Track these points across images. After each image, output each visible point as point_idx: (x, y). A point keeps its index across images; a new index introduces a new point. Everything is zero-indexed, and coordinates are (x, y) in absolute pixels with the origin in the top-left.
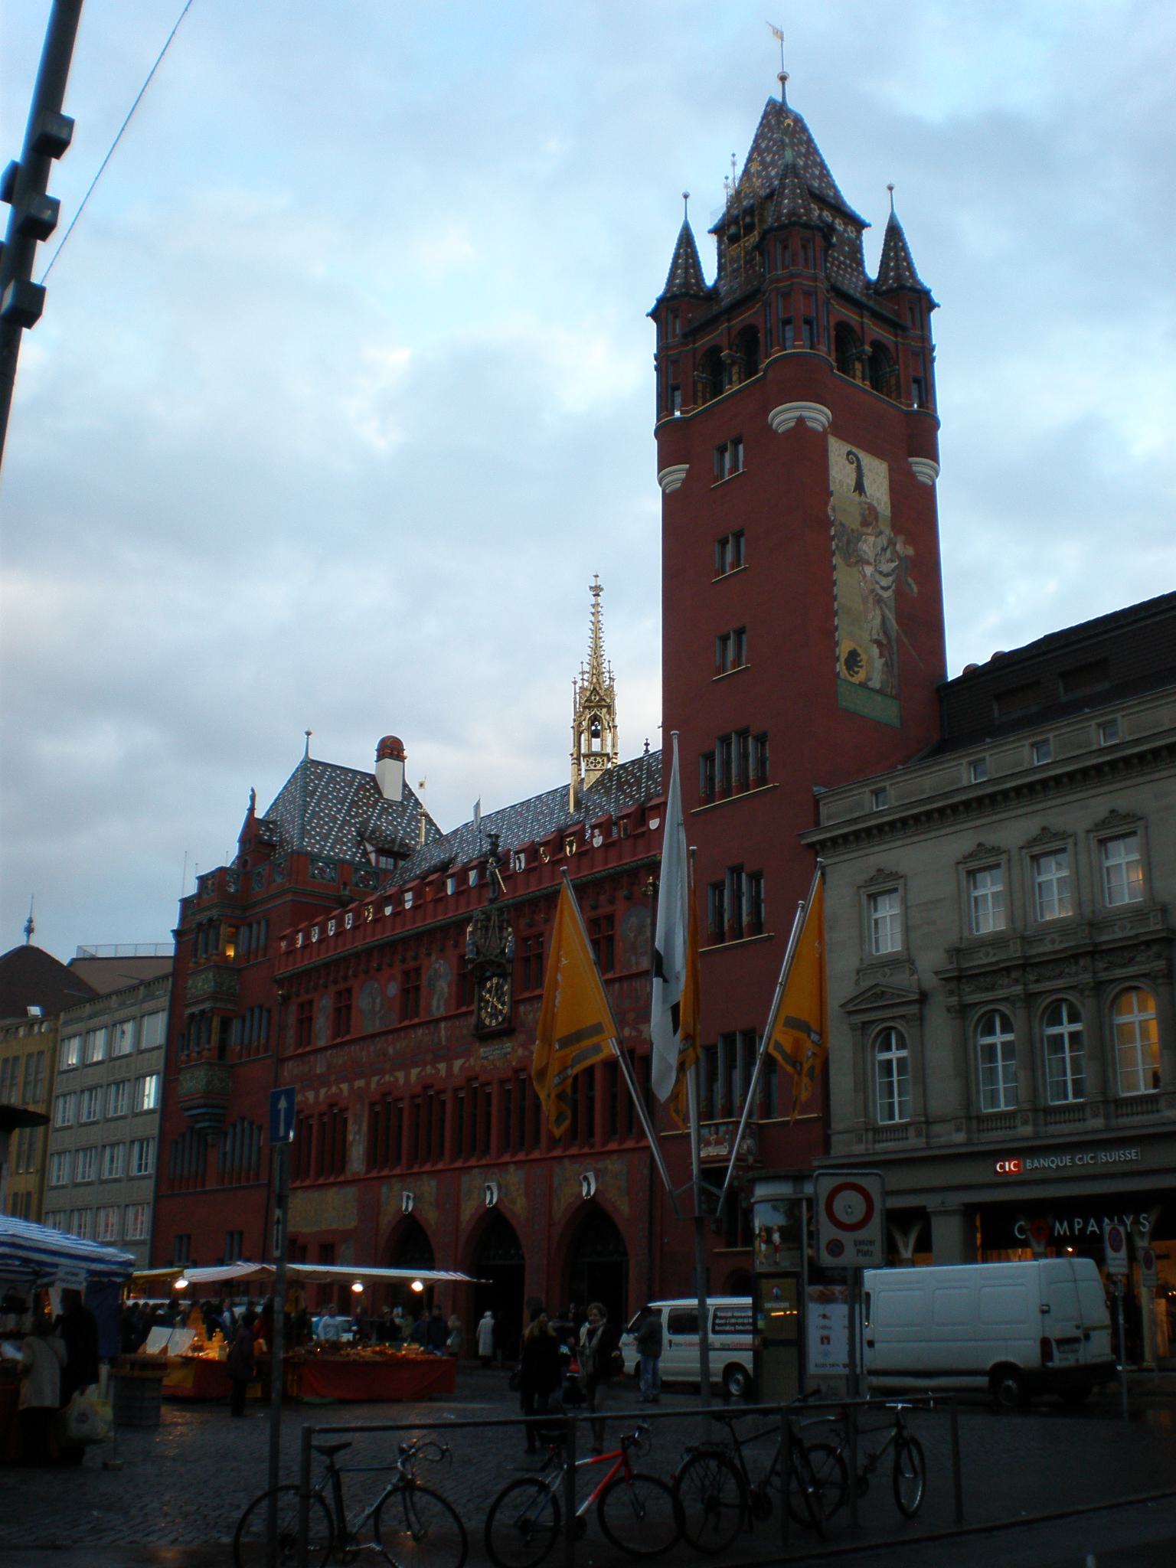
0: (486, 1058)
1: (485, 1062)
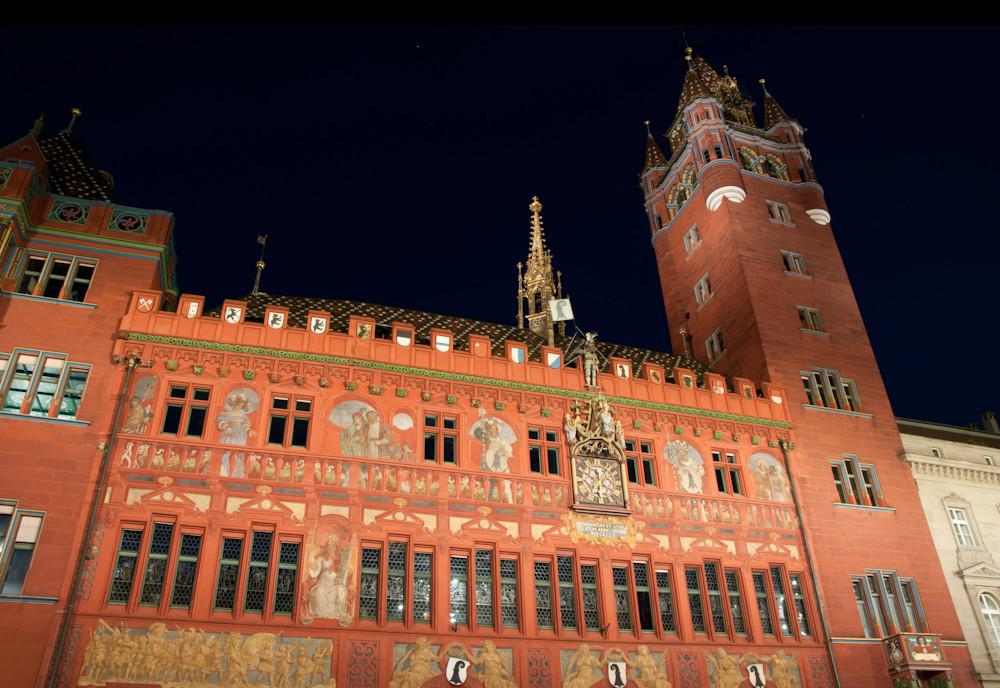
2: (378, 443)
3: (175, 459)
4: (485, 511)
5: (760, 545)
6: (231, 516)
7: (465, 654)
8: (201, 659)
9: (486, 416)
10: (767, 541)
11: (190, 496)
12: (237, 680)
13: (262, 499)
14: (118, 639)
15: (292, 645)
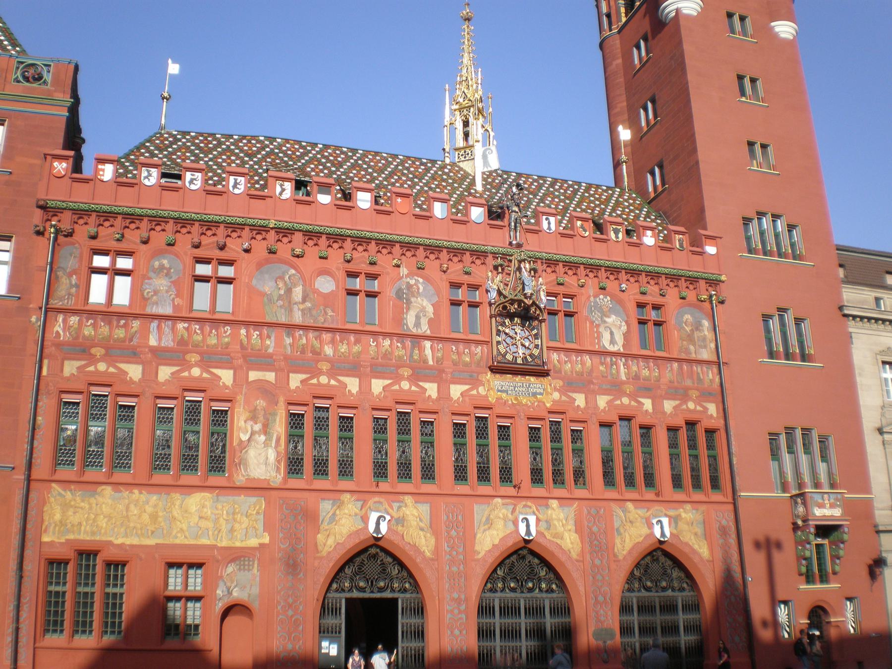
0: (506, 392)
1: (504, 395)
2: (301, 307)
3: (104, 330)
4: (406, 372)
5: (677, 402)
6: (164, 384)
7: (385, 509)
8: (146, 518)
9: (407, 276)
10: (685, 398)
11: (123, 366)
12: (179, 535)
13: (189, 367)
14: (70, 501)
15: (227, 502)
